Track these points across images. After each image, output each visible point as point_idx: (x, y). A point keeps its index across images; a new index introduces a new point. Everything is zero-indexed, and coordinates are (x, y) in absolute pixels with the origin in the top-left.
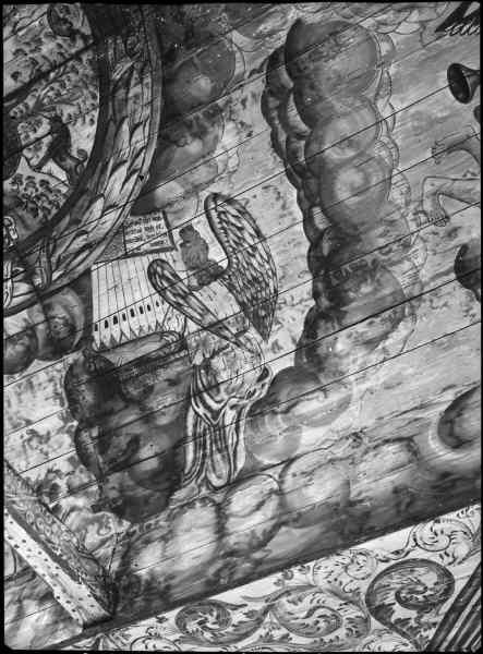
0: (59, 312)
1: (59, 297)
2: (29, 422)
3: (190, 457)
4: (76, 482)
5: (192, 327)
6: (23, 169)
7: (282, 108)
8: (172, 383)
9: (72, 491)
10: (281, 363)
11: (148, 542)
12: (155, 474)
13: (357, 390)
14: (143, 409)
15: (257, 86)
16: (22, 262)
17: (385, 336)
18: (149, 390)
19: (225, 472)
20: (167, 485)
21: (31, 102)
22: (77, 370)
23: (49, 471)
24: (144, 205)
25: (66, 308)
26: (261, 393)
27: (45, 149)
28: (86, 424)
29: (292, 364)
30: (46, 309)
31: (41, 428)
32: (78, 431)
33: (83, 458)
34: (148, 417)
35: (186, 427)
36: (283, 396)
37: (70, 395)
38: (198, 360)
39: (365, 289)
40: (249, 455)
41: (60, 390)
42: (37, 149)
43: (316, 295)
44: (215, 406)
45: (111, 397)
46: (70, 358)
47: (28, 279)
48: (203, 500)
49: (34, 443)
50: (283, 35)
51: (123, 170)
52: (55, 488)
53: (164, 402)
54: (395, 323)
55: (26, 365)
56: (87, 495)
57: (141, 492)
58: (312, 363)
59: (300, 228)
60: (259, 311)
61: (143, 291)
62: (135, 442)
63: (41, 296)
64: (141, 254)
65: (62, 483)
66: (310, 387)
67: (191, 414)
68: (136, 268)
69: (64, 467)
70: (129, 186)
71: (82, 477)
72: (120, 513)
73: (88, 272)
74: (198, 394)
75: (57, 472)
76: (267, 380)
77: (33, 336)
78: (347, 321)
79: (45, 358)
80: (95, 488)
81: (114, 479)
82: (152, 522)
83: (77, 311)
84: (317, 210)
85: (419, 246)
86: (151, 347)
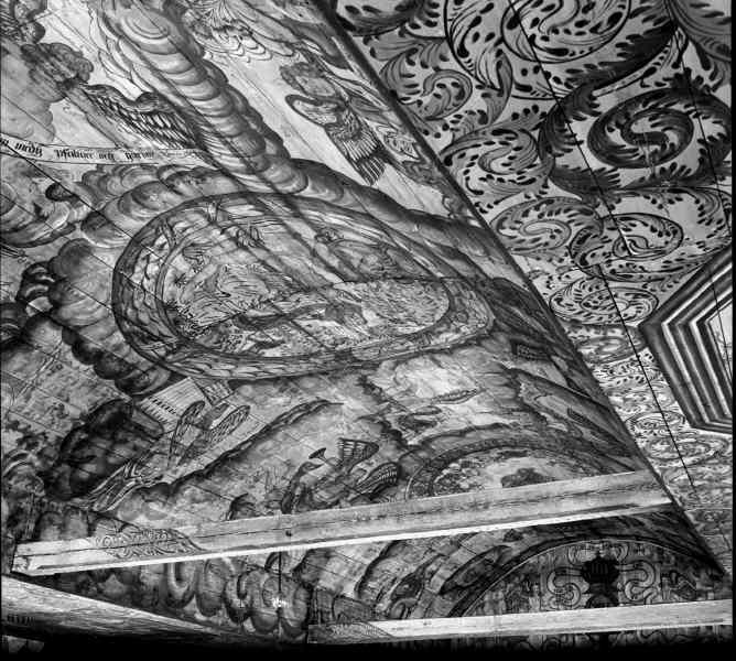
0: (152, 375)
1: (163, 371)
2: (67, 401)
3: (100, 487)
4: (47, 452)
5: (170, 436)
6: (246, 333)
7: (300, 411)
8: (135, 448)
9: (40, 454)
10: (168, 480)
11: (51, 522)
12: (82, 482)
13: (172, 514)
14: (112, 447)
15: (310, 399)
16: (179, 347)
17: (198, 502)
18: (125, 442)
19: (102, 506)
20: (77, 490)
21: (294, 332)
22: (118, 404)
23: (44, 434)
24: (235, 384)
25: (156, 379)
26: (149, 485)
27: (263, 340)
28: (86, 429)
29: (170, 483)
30: (153, 369)
31: (69, 409)
32: (79, 428)
33: (64, 443)
34: (108, 453)
35: (114, 471)
36: (153, 494)
37: (98, 410)
38: (153, 450)
39: (217, 480)
40: (117, 508)
41: (100, 404)
42: (262, 337)
43: (207, 467)
44: (133, 475)
45: (109, 428)
46: (124, 396)
47: (168, 353)
48: (84, 513)
49: (55, 412)
50: (336, 401)
51: (256, 370)
52: (36, 444)
53: (123, 451)
54: (207, 500)
55: (107, 378)
56: (44, 463)
57: (66, 485)
58: (170, 492)
59: (239, 442)
60: (191, 453)
61: (181, 406)
62: (91, 458)
63: (160, 363)
64: (205, 395)
65: (41, 445)
66: (163, 499)
67: (122, 469)
68: (199, 396)
69: (51, 439)
70: (246, 375)
71: (51, 452)
72: (47, 485)
73: (186, 377)
74: (135, 462)
75: (46, 438)
76: (157, 482)
77: (129, 371)
78: (200, 485)
79: (117, 385)
80: (51, 463)
81: (65, 467)
82: (55, 504)
83: (157, 384)
84: (250, 443)
85: (243, 481)
86: (150, 426)
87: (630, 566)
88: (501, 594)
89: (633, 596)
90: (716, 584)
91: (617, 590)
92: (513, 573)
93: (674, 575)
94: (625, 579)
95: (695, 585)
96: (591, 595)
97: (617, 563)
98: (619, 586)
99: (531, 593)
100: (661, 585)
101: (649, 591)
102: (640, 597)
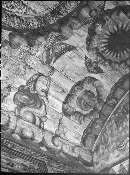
88: (113, 121)
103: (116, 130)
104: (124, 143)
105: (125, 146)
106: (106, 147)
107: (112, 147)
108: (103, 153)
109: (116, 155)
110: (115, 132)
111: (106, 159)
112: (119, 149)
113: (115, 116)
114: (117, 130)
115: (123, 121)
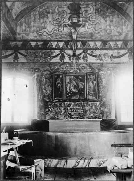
87: (85, 6)
88: (37, 12)
89: (86, 15)
90: (113, 14)
91: (80, 13)
92: (42, 5)
93: (100, 10)
94: (83, 10)
95: (106, 13)
96: (71, 14)
97: (81, 5)
98: (81, 12)
99: (49, 13)
100: (95, 13)
101: (91, 14)
102: (88, 16)
103: (38, 20)
104: (42, 31)
105: (42, 33)
106: (28, 27)
107: (33, 29)
108: (25, 30)
109: (35, 35)
110: (37, 20)
111: (27, 35)
112: (38, 33)
113: (39, 10)
114: (39, 20)
115: (44, 17)
